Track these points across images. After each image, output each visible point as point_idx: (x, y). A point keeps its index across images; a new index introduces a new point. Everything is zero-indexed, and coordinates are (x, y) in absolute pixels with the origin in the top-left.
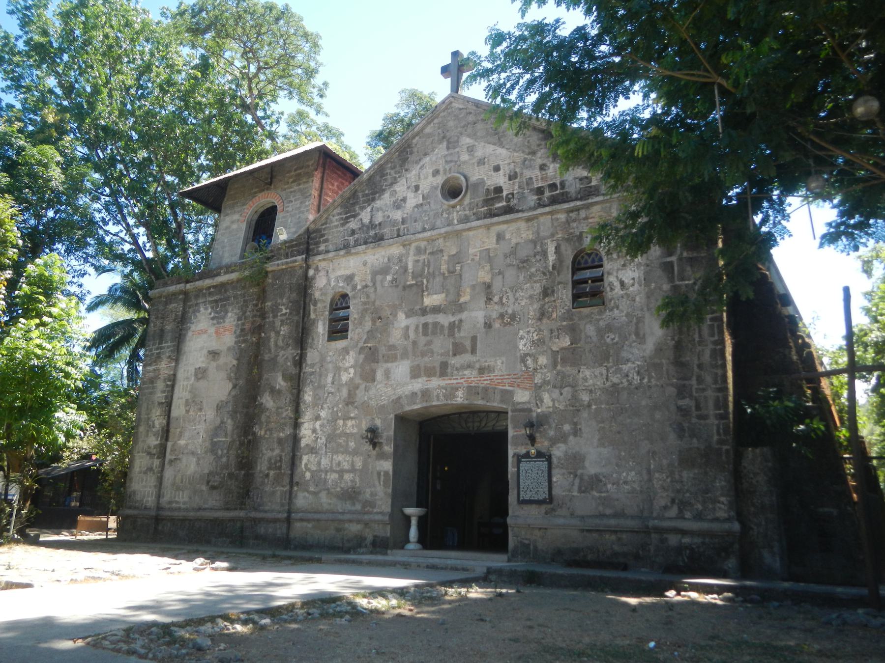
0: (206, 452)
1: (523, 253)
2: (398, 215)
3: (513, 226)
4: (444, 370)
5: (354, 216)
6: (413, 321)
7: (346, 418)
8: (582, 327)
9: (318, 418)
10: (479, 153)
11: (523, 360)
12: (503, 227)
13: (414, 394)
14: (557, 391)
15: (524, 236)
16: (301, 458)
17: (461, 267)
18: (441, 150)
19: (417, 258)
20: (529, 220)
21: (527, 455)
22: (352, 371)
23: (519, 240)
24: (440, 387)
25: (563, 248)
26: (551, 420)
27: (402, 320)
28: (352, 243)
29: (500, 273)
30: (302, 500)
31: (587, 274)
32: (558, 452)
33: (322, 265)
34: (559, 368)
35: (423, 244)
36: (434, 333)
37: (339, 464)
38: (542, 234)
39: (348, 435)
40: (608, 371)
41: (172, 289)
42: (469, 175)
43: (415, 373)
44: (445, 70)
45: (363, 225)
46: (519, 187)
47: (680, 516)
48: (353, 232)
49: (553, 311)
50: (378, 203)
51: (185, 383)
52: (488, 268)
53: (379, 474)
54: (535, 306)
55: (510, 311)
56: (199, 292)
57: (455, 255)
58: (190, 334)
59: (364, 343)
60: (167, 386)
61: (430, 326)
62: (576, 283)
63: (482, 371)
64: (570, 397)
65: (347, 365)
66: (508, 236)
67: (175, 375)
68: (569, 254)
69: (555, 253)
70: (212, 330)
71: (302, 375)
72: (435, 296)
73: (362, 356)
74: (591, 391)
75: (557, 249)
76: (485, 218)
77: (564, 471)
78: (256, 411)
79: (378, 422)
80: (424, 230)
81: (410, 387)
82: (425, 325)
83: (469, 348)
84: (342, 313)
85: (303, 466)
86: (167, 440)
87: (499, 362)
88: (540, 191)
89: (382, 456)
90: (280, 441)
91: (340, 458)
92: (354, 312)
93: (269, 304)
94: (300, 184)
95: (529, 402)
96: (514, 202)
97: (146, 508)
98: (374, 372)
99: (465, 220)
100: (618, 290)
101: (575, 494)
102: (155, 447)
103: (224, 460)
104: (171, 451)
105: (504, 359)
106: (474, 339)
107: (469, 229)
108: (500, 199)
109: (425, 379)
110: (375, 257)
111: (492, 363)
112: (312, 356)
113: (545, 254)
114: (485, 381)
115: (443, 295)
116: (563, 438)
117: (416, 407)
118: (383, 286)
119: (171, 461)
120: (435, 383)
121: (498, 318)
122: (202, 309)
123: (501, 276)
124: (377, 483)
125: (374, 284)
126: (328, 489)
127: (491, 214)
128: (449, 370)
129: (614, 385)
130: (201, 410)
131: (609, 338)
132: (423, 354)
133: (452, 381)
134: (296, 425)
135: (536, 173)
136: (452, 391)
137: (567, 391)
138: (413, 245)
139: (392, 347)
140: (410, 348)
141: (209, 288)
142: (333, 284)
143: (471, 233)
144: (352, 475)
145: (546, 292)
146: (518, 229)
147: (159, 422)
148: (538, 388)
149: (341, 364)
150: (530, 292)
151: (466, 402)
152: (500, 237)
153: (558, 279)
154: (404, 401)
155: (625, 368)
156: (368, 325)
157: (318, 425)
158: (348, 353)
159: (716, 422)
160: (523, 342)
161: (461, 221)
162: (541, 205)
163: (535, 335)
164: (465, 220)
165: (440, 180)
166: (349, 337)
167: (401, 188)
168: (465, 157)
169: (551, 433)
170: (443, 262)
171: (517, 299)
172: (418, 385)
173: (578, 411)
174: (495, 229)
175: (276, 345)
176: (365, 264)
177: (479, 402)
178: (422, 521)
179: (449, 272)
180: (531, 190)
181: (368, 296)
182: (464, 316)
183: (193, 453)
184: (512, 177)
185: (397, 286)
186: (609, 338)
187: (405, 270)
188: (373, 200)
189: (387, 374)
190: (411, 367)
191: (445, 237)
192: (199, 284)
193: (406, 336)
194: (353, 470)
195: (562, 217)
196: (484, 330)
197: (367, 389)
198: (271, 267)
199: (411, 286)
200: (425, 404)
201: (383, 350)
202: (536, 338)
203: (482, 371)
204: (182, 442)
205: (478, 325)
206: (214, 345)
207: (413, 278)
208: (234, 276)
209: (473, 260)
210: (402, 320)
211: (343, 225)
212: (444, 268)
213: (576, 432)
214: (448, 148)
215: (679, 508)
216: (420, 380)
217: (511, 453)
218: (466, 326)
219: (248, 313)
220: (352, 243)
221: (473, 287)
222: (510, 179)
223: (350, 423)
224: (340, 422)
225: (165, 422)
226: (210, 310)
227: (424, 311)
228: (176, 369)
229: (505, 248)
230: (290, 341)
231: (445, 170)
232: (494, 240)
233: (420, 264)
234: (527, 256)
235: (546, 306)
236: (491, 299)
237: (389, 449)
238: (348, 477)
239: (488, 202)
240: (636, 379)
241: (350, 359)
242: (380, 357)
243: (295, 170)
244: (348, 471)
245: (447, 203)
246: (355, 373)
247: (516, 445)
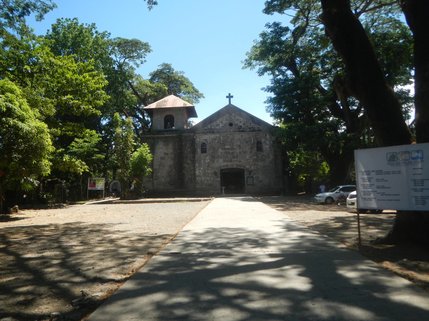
2: (218, 128)
4: (231, 161)
5: (206, 126)
6: (223, 151)
7: (208, 170)
9: (200, 170)
10: (237, 118)
11: (247, 160)
12: (242, 134)
13: (224, 166)
16: (196, 178)
18: (228, 115)
20: (248, 134)
21: (249, 177)
22: (209, 160)
27: (220, 150)
28: (206, 132)
30: (198, 186)
31: (259, 145)
32: (254, 176)
33: (198, 136)
35: (224, 135)
41: (149, 136)
44: (227, 97)
45: (208, 129)
48: (206, 130)
50: (212, 124)
56: (158, 138)
58: (156, 148)
59: (212, 154)
62: (257, 147)
63: (239, 162)
66: (244, 136)
68: (256, 142)
73: (211, 157)
75: (254, 140)
76: (238, 132)
79: (216, 171)
80: (224, 132)
82: (226, 152)
88: (250, 128)
89: (218, 177)
90: (191, 174)
91: (207, 178)
92: (208, 147)
93: (183, 144)
96: (245, 129)
99: (234, 131)
100: (265, 149)
103: (173, 178)
106: (237, 156)
108: (242, 128)
110: (213, 136)
112: (197, 156)
113: (251, 141)
114: (240, 163)
117: (225, 168)
120: (229, 163)
122: (160, 142)
125: (213, 142)
130: (164, 167)
131: (263, 157)
134: (195, 171)
135: (249, 125)
136: (233, 165)
138: (222, 135)
141: (162, 137)
142: (201, 140)
145: (252, 148)
148: (251, 165)
152: (242, 136)
155: (266, 162)
156: (212, 151)
157: (200, 171)
162: (250, 131)
164: (234, 131)
165: (227, 122)
167: (218, 122)
168: (233, 118)
169: (253, 173)
172: (225, 164)
175: (187, 153)
176: (210, 137)
177: (239, 167)
178: (225, 189)
182: (235, 151)
183: (163, 177)
184: (244, 124)
186: (263, 157)
187: (220, 140)
188: (211, 123)
189: (218, 161)
192: (158, 136)
193: (222, 153)
194: (211, 180)
195: (254, 134)
198: (184, 134)
203: (239, 162)
204: (159, 174)
206: (166, 152)
208: (171, 135)
210: (220, 150)
211: (203, 127)
212: (230, 141)
214: (229, 115)
217: (245, 176)
219: (176, 145)
220: (206, 132)
221: (236, 145)
223: (209, 171)
224: (207, 171)
227: (225, 149)
232: (240, 136)
237: (219, 176)
239: (238, 128)
240: (268, 164)
241: (208, 158)
245: (230, 127)
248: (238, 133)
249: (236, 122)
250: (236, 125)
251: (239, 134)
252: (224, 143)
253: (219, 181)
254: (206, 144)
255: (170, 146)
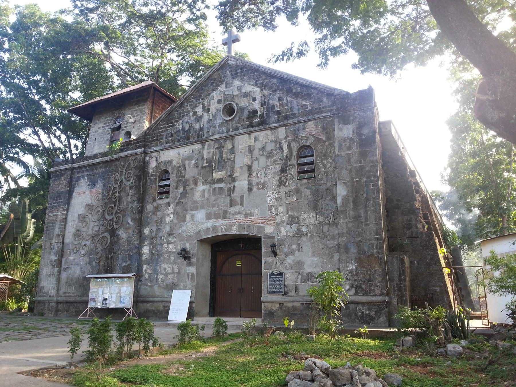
0: (86, 264)
1: (270, 147)
3: (264, 133)
4: (225, 215)
6: (206, 187)
7: (169, 243)
8: (302, 190)
11: (270, 209)
13: (208, 229)
14: (289, 226)
15: (270, 138)
17: (235, 156)
19: (209, 151)
20: (272, 129)
22: (172, 216)
23: (267, 141)
24: (223, 225)
25: (292, 145)
26: (285, 243)
27: (201, 187)
29: (257, 159)
31: (305, 160)
34: (290, 213)
36: (220, 194)
37: (165, 269)
38: (280, 137)
39: (170, 253)
40: (317, 215)
42: (239, 103)
43: (208, 217)
46: (267, 110)
47: (356, 293)
48: (172, 135)
49: (286, 181)
51: (72, 223)
52: (249, 157)
53: (188, 275)
54: (276, 179)
55: (262, 181)
57: (230, 149)
58: (74, 194)
60: (62, 225)
61: (217, 190)
64: (296, 229)
65: (169, 212)
66: (261, 139)
67: (66, 218)
69: (288, 148)
70: (87, 192)
71: (143, 218)
72: (220, 173)
74: (307, 226)
76: (247, 128)
77: (292, 271)
78: (116, 240)
79: (188, 246)
81: (206, 225)
82: (214, 189)
83: (239, 202)
84: (165, 183)
85: (144, 271)
86: (62, 256)
87: (256, 210)
89: (190, 264)
94: (139, 106)
95: (273, 233)
97: (50, 296)
98: (185, 216)
101: (299, 283)
102: (55, 260)
104: (65, 263)
105: (259, 209)
106: (242, 197)
107: (239, 134)
109: (214, 220)
110: (185, 151)
111: (252, 211)
113: (281, 148)
114: (248, 221)
115: (224, 172)
116: (292, 253)
118: (190, 167)
119: (65, 269)
120: (220, 222)
121: (255, 185)
123: (257, 161)
124: (187, 280)
126: (159, 284)
127: (251, 126)
128: (228, 215)
129: (320, 223)
132: (213, 206)
133: (230, 221)
134: (140, 248)
137: (294, 226)
139: (195, 202)
140: (205, 202)
143: (240, 137)
144: (172, 276)
145: (283, 170)
146: (267, 134)
147: (57, 246)
148: (278, 225)
149: (165, 212)
150: (274, 171)
151: (238, 233)
152: (256, 139)
153: (289, 163)
154: (202, 233)
158: (170, 206)
159: (376, 242)
160: (269, 199)
161: (233, 130)
163: (276, 195)
165: (221, 106)
166: (170, 196)
169: (286, 250)
170: (224, 153)
171: (266, 175)
172: (210, 224)
173: (301, 237)
174: (253, 135)
176: (179, 154)
179: (228, 159)
180: (274, 112)
181: (181, 173)
182: (236, 184)
183: (78, 264)
185: (197, 167)
187: (203, 158)
189: (192, 217)
190: (206, 213)
191: (225, 139)
193: (203, 196)
196: (247, 192)
197: (181, 227)
199: (205, 167)
200: (214, 235)
201: (190, 204)
202: (277, 196)
203: (246, 215)
205: (244, 189)
207: (207, 162)
209: (241, 152)
210: (201, 187)
213: (299, 249)
214: (226, 87)
215: (356, 290)
216: (211, 221)
218: (237, 190)
222: (262, 106)
223: (171, 246)
224: (166, 245)
225: (60, 246)
226: (87, 180)
228: (67, 215)
229: (259, 145)
230: (135, 199)
231: (224, 100)
232: (253, 141)
233: (211, 154)
234: (272, 150)
235: (283, 179)
236: (252, 174)
238: (170, 276)
242: (189, 208)
243: (137, 98)
244: (169, 274)
246: (174, 217)
247: (266, 257)
248: (245, 131)
249: (243, 102)
250: (242, 109)
251: (249, 133)
252: (210, 166)
253: (192, 274)
254: (170, 172)
255: (100, 185)
